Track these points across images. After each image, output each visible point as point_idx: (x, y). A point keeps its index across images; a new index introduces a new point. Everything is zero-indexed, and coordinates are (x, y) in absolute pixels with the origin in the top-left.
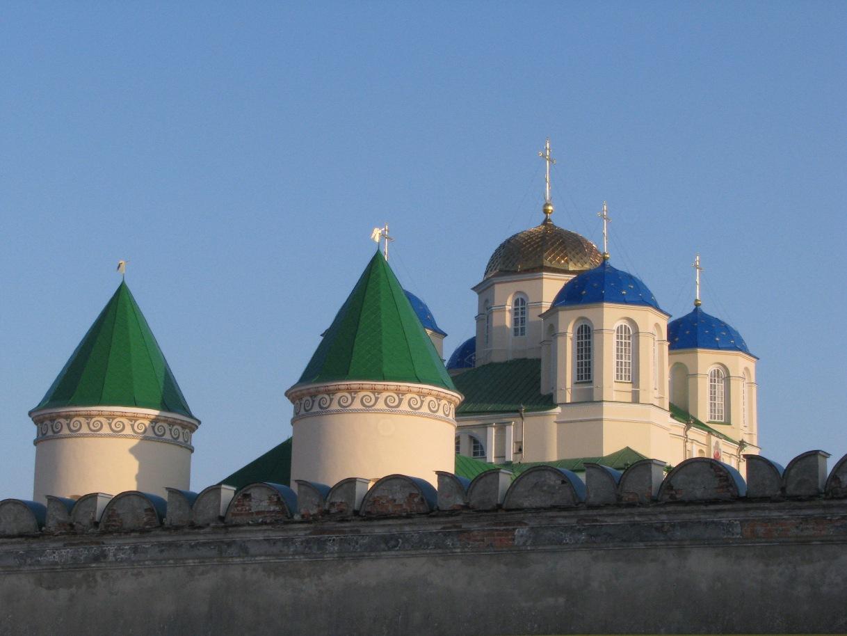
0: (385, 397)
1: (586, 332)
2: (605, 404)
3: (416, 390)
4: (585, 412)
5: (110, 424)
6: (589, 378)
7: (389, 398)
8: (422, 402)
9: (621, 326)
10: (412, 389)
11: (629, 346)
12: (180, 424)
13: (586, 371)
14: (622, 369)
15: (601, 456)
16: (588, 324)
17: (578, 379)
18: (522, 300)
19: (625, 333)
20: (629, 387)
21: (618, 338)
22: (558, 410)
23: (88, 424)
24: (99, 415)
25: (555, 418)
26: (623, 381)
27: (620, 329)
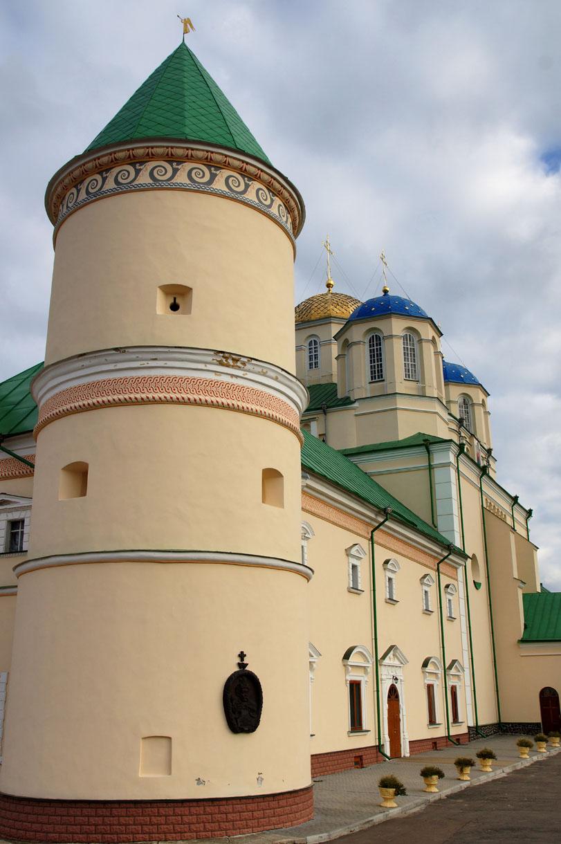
1: (376, 341)
3: (237, 163)
6: (382, 377)
7: (194, 171)
8: (247, 186)
9: (406, 335)
10: (231, 161)
13: (377, 374)
15: (397, 440)
17: (372, 379)
18: (314, 341)
22: (356, 405)
27: (405, 338)
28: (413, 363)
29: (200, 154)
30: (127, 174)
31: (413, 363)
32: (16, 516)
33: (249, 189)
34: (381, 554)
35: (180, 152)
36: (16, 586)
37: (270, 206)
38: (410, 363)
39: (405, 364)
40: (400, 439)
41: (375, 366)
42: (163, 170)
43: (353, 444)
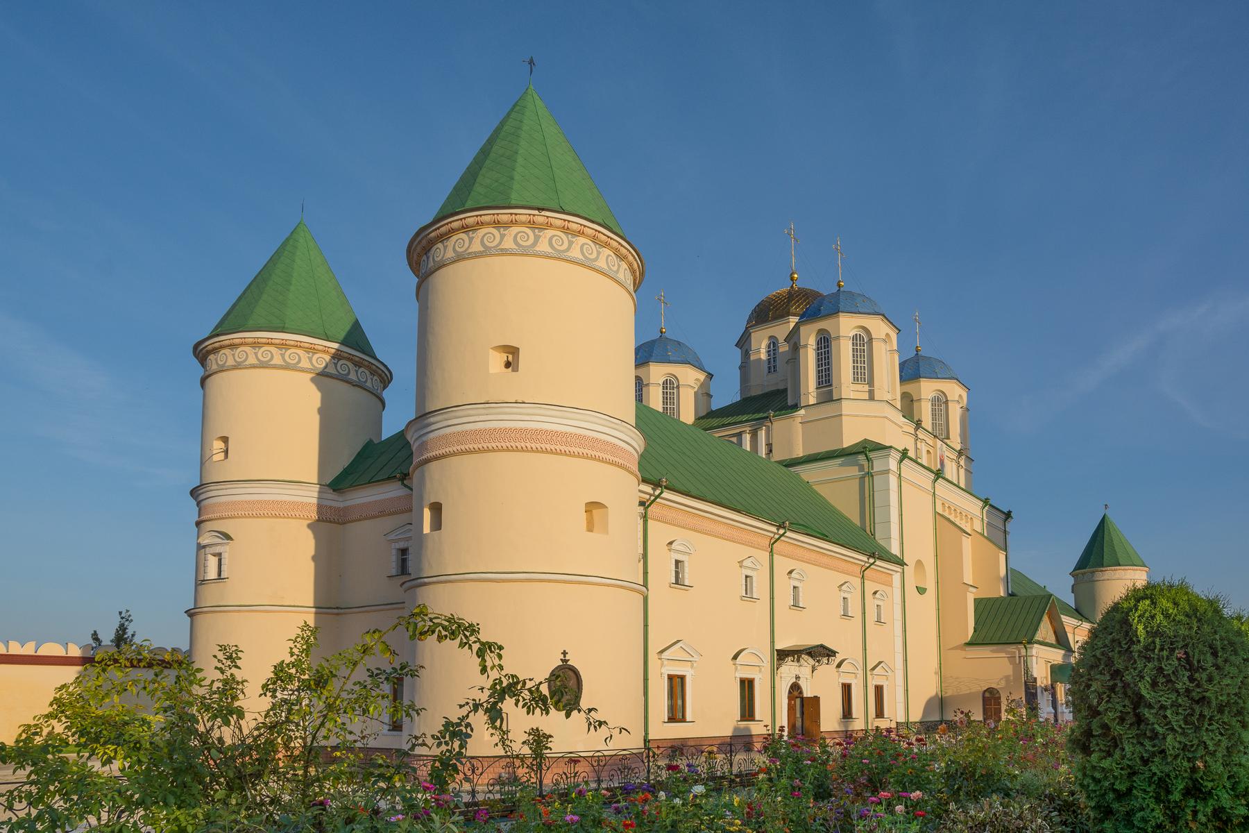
0: (513, 234)
1: (824, 343)
2: (844, 402)
3: (559, 223)
4: (828, 409)
5: (256, 354)
7: (518, 237)
8: (571, 243)
9: (856, 335)
11: (864, 358)
12: (348, 359)
13: (826, 378)
14: (857, 372)
16: (826, 336)
17: (819, 384)
19: (860, 341)
20: (866, 388)
21: (853, 346)
22: (802, 412)
23: (233, 355)
24: (242, 344)
25: (799, 420)
26: (859, 382)
27: (855, 338)
28: (862, 365)
29: (523, 218)
30: (461, 241)
31: (862, 365)
32: (402, 545)
33: (573, 246)
34: (782, 564)
35: (505, 218)
36: (404, 603)
37: (596, 259)
38: (859, 365)
39: (854, 366)
40: (844, 446)
41: (822, 370)
42: (492, 236)
43: (799, 452)
